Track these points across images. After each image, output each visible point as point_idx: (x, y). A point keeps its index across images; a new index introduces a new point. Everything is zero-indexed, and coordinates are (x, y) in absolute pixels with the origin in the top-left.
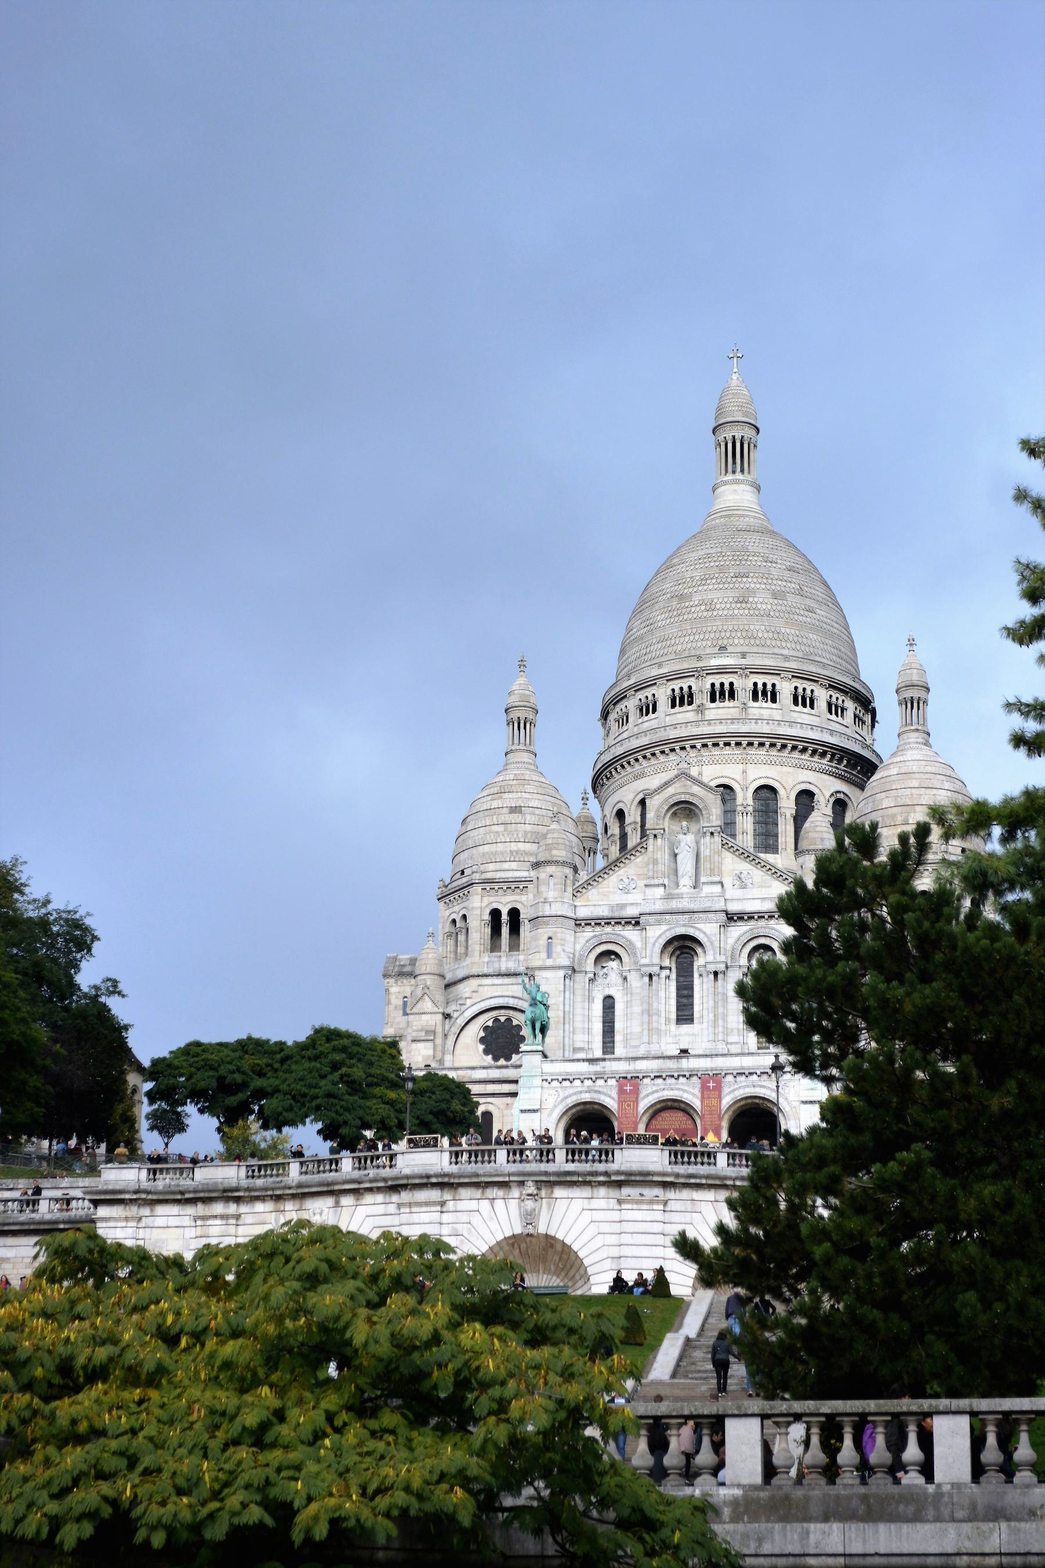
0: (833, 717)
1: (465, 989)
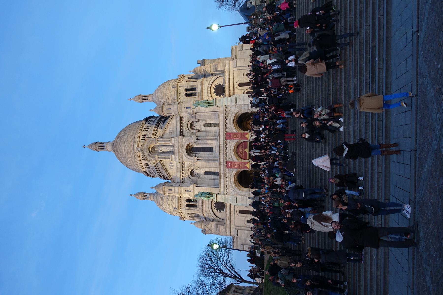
0: (152, 122)
1: (206, 215)
